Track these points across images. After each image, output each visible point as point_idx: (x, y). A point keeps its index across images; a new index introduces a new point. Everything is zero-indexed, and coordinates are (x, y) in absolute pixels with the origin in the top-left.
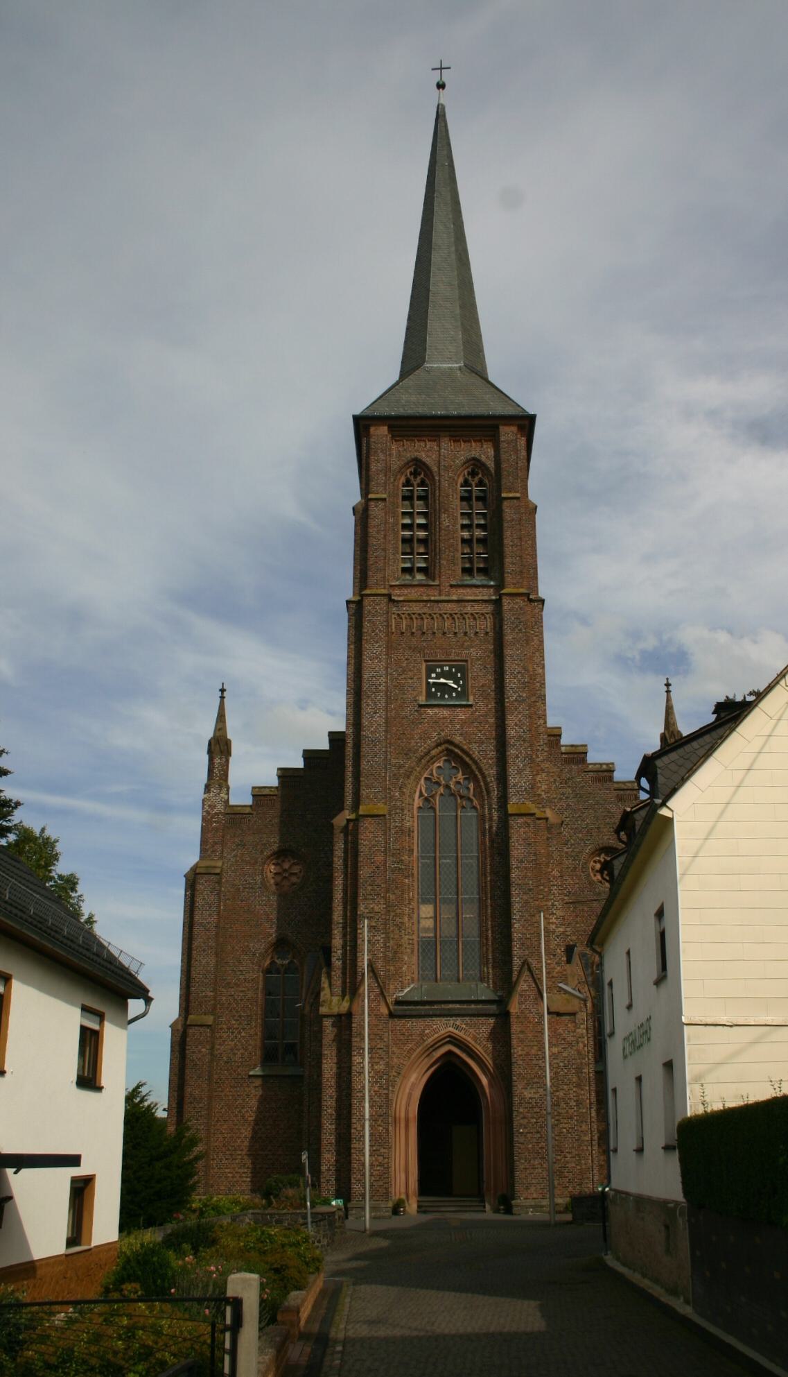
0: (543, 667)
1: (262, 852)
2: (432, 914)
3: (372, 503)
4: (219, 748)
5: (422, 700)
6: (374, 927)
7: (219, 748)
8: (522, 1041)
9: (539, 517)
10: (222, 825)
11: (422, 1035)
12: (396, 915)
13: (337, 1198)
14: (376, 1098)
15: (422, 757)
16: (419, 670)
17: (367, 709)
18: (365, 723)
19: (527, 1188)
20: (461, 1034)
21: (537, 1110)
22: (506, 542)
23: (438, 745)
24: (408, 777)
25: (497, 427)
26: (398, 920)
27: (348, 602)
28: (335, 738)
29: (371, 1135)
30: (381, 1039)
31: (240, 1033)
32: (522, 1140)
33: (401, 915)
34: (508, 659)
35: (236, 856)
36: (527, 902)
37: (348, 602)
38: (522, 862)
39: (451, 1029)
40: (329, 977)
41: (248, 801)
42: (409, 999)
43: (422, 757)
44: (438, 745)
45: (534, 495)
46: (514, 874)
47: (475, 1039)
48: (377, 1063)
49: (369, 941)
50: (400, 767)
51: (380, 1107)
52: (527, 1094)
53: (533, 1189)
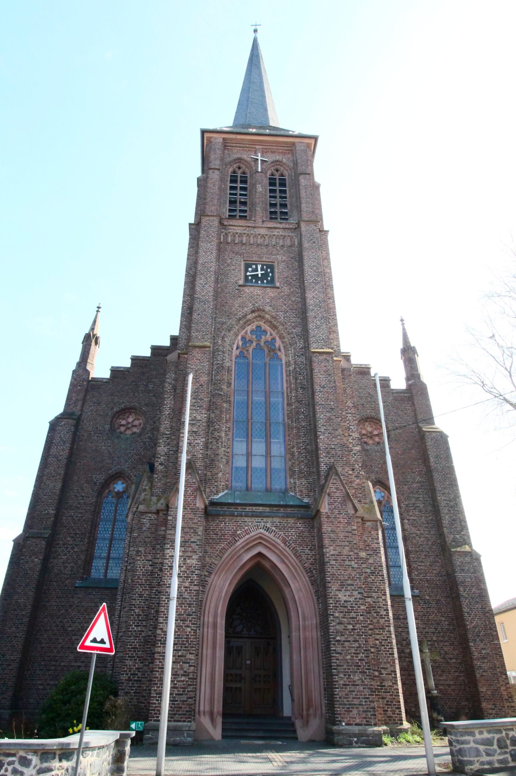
0: (330, 269)
1: (112, 408)
2: (244, 452)
3: (211, 171)
4: (90, 340)
5: (241, 282)
6: (195, 432)
7: (90, 340)
8: (333, 541)
9: (322, 190)
10: (83, 385)
11: (234, 534)
12: (215, 430)
13: (136, 720)
14: (186, 595)
15: (240, 319)
16: (240, 265)
17: (200, 281)
18: (198, 289)
19: (349, 711)
20: (271, 536)
21: (353, 615)
22: (302, 195)
23: (253, 312)
24: (229, 331)
25: (237, 468)
26: (216, 434)
27: (190, 224)
28: (174, 339)
29: (177, 637)
30: (195, 532)
31: (73, 548)
32: (339, 649)
33: (219, 430)
34: (305, 258)
35: (92, 410)
36: (330, 419)
37: (190, 224)
38: (324, 387)
39: (262, 531)
40: (151, 480)
41: (107, 375)
42: (223, 501)
43: (240, 319)
44: (253, 312)
45: (318, 178)
46: (319, 397)
47: (285, 542)
48: (190, 557)
49: (189, 444)
50: (223, 323)
51: (190, 605)
52: (342, 596)
53: (355, 711)
